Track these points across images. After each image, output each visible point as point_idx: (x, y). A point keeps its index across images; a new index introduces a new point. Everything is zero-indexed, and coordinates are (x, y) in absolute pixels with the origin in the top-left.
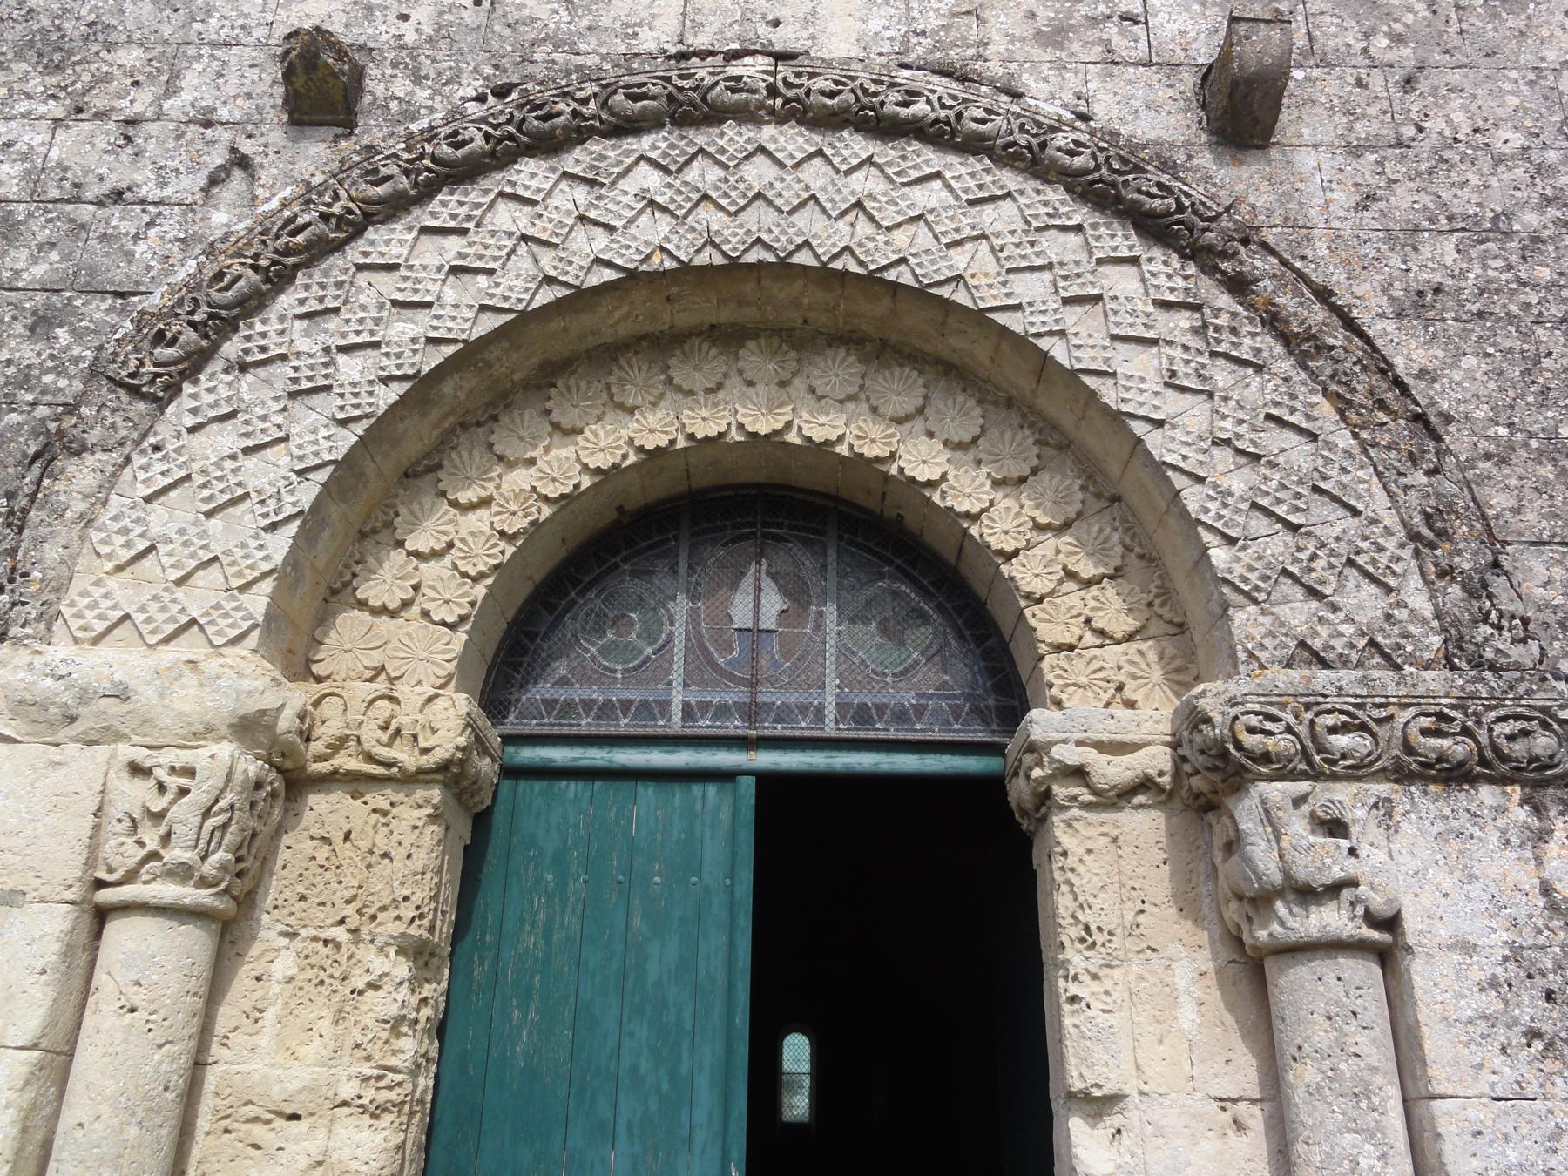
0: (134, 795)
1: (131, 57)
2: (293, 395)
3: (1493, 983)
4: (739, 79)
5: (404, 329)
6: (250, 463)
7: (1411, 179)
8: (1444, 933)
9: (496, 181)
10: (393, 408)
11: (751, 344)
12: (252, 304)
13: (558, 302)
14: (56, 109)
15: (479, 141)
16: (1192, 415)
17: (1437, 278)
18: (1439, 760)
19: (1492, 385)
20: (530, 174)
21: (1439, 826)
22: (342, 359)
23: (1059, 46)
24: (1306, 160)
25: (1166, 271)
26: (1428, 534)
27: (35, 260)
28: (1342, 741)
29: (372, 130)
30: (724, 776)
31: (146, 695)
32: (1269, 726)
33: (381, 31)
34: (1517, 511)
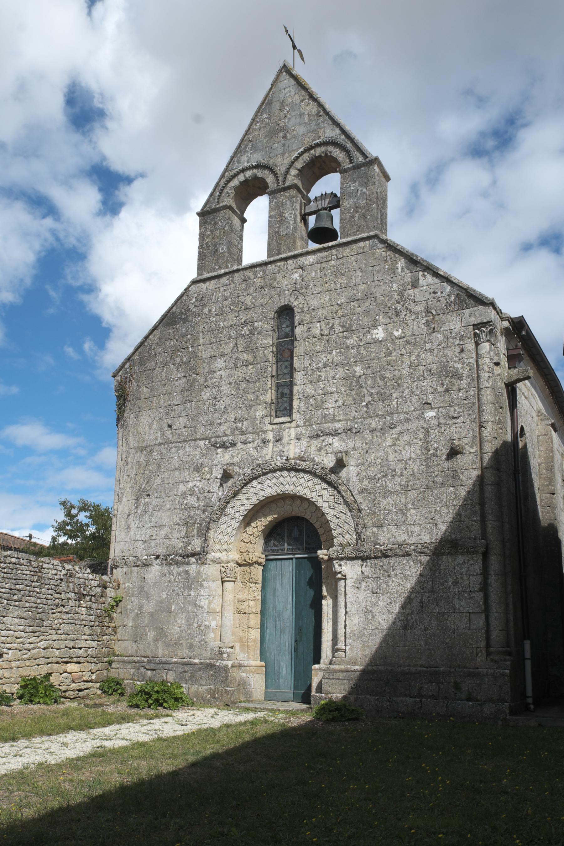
0: (223, 569)
5: (243, 508)
6: (228, 529)
8: (350, 577)
9: (250, 485)
12: (225, 507)
14: (199, 479)
16: (332, 512)
17: (364, 487)
20: (254, 483)
23: (320, 451)
25: (330, 490)
28: (340, 556)
30: (291, 559)
31: (222, 558)
33: (236, 460)
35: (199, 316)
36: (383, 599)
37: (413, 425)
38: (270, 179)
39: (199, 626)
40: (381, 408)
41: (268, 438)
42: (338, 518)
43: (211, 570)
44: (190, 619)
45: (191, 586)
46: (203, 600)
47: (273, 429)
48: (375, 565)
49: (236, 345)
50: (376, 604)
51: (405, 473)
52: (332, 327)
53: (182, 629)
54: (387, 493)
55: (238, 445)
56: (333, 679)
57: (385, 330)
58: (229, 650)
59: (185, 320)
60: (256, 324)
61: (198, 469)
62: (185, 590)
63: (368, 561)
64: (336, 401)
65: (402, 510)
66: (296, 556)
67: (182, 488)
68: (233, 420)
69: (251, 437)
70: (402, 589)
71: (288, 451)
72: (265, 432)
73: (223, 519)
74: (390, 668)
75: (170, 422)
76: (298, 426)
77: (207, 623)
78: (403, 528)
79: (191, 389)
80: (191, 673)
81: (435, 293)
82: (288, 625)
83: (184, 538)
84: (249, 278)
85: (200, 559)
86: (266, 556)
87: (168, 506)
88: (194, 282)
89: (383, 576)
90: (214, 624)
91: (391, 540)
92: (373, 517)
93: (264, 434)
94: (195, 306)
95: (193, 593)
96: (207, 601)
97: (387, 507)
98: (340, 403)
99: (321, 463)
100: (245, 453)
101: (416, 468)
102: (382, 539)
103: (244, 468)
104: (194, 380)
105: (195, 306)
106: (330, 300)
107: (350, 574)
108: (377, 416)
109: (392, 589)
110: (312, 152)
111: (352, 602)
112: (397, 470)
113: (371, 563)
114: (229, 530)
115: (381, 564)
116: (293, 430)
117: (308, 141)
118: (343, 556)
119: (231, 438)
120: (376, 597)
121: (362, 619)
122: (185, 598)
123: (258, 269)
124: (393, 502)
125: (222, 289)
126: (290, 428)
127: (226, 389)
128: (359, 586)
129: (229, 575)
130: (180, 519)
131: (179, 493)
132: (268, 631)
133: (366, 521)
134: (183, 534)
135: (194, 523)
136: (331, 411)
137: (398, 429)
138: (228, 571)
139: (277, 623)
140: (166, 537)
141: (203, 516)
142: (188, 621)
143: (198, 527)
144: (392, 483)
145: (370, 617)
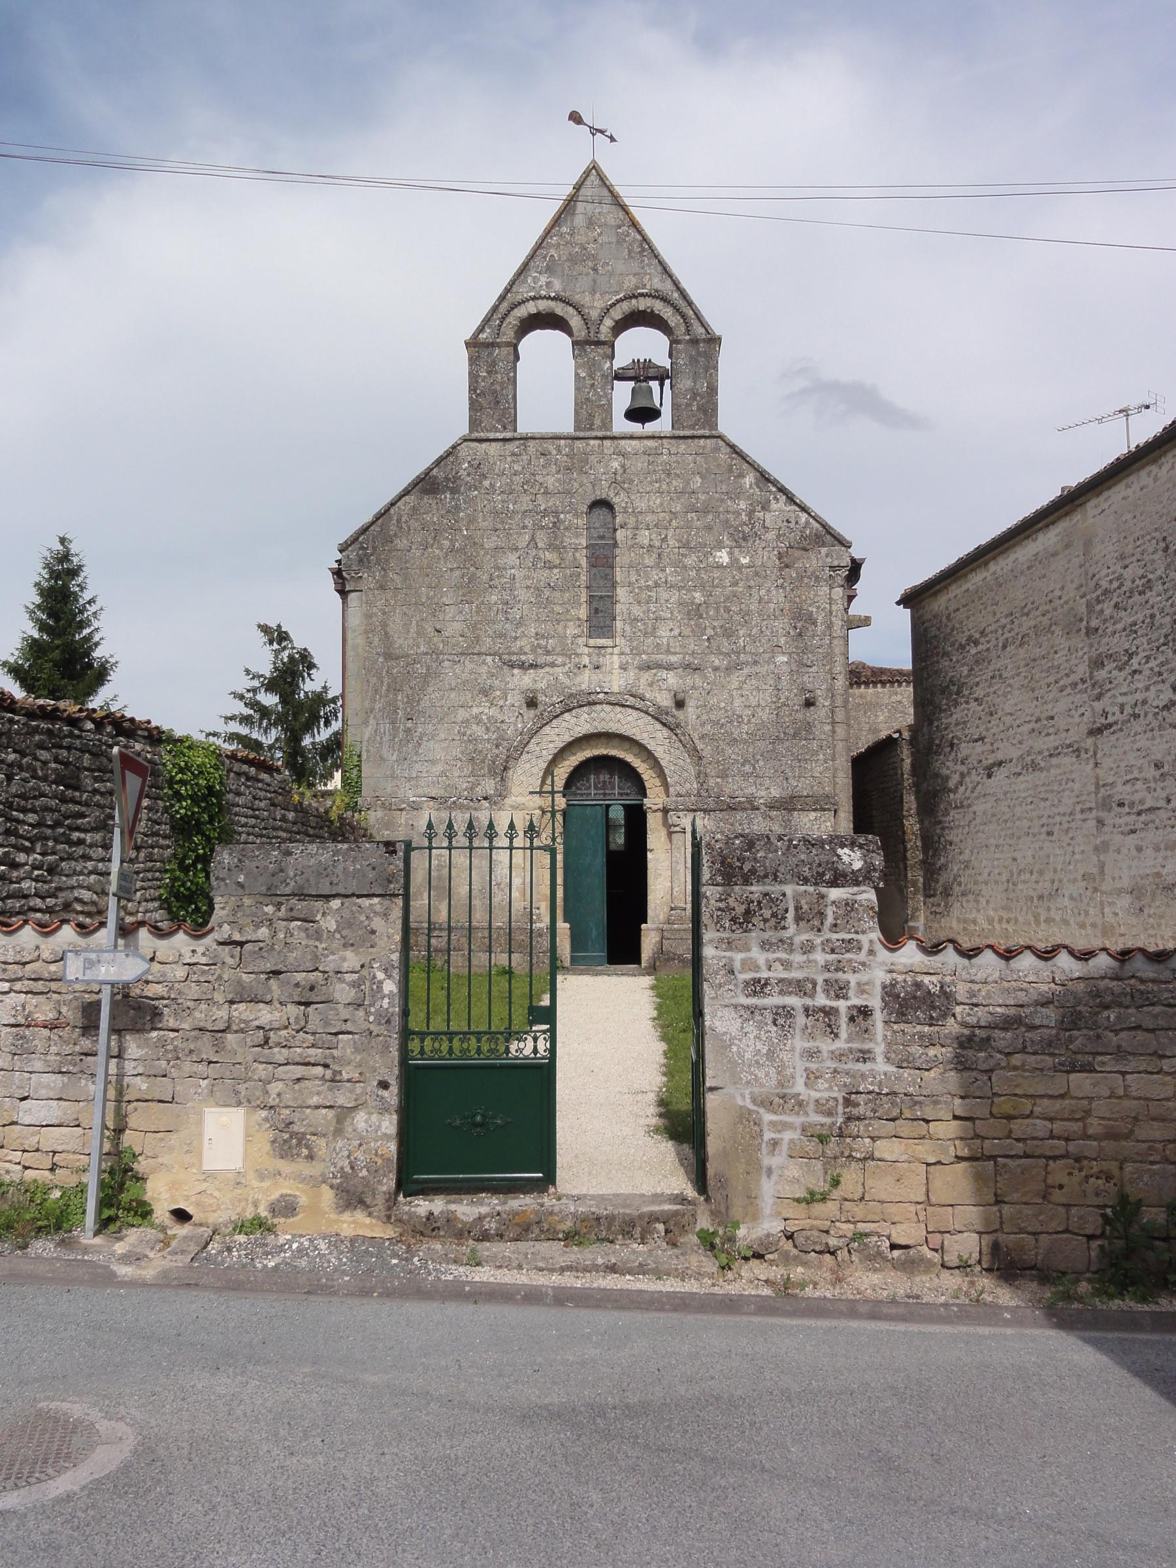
1: (498, 693)
5: (551, 745)
16: (668, 757)
20: (567, 716)
24: (690, 709)
25: (666, 732)
26: (698, 776)
29: (541, 708)
35: (476, 489)
37: (762, 669)
38: (575, 322)
40: (726, 646)
49: (533, 538)
51: (753, 720)
52: (664, 540)
57: (730, 554)
59: (454, 491)
60: (562, 516)
61: (485, 692)
64: (671, 630)
67: (462, 714)
69: (560, 660)
72: (577, 655)
73: (525, 757)
75: (438, 627)
76: (622, 653)
79: (469, 589)
81: (788, 521)
84: (550, 453)
87: (443, 736)
88: (465, 440)
94: (469, 475)
98: (676, 632)
101: (765, 717)
104: (474, 575)
105: (469, 475)
106: (661, 504)
108: (721, 653)
110: (634, 301)
116: (615, 657)
117: (630, 283)
123: (562, 442)
125: (509, 459)
126: (612, 654)
127: (522, 594)
130: (462, 753)
134: (466, 772)
136: (665, 641)
137: (746, 671)
140: (443, 774)
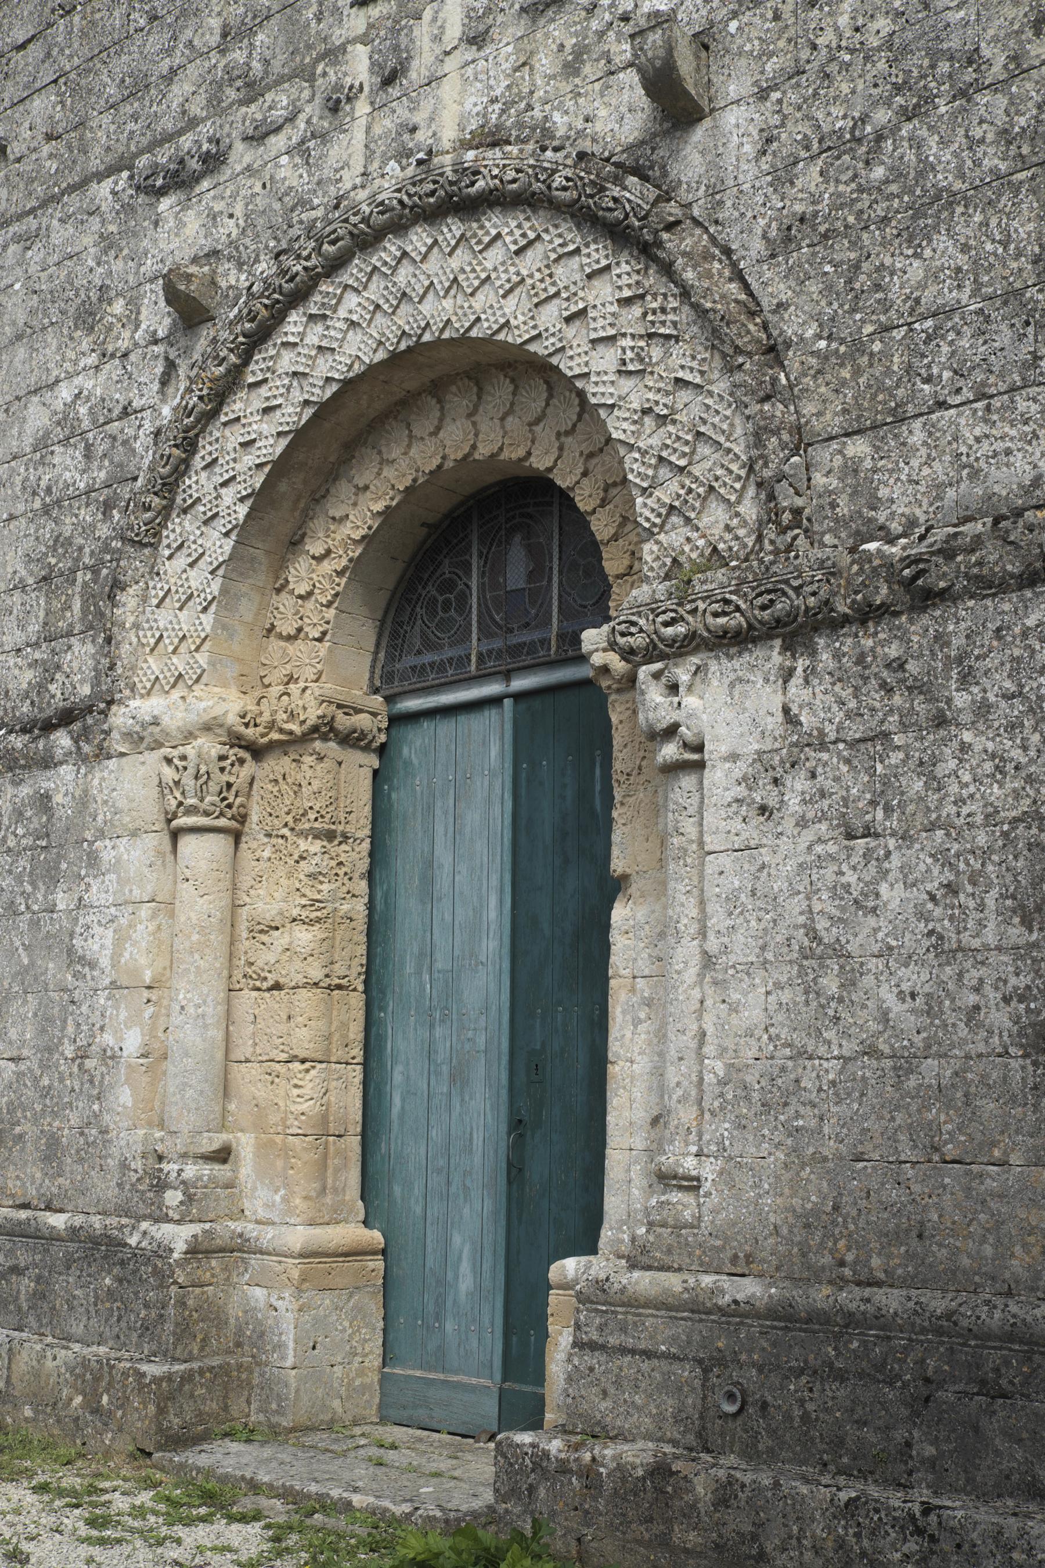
0: (169, 774)
2: (206, 523)
3: (745, 778)
4: (382, 203)
7: (799, 108)
8: (724, 749)
10: (248, 516)
11: (454, 389)
13: (315, 415)
15: (264, 312)
16: (636, 394)
17: (799, 208)
18: (726, 633)
19: (823, 303)
20: (295, 319)
21: (733, 676)
22: (223, 491)
23: (577, 73)
25: (626, 270)
27: (100, 469)
28: (669, 631)
30: (495, 701)
32: (633, 630)
34: (820, 414)
36: (905, 870)
39: (82, 1055)
41: (348, 81)
42: (662, 420)
43: (129, 784)
44: (50, 1020)
45: (57, 868)
46: (97, 930)
47: (371, 26)
48: (860, 660)
50: (866, 903)
53: (23, 1067)
54: (928, 208)
55: (232, 158)
56: (624, 1351)
58: (191, 1171)
62: (35, 887)
63: (821, 642)
65: (1018, 293)
66: (521, 683)
68: (214, 39)
70: (1017, 795)
71: (432, 119)
74: (938, 1303)
77: (108, 1039)
78: (1022, 405)
80: (38, 1279)
82: (481, 1041)
83: (36, 645)
85: (85, 734)
86: (389, 699)
89: (904, 728)
90: (132, 1041)
91: (951, 493)
92: (846, 373)
93: (335, 63)
95: (62, 901)
96: (110, 933)
97: (927, 296)
99: (581, 134)
100: (258, 188)
102: (900, 499)
103: (257, 260)
107: (722, 730)
109: (960, 801)
111: (732, 899)
112: (986, 52)
113: (837, 656)
114: (196, 578)
115: (893, 651)
118: (681, 629)
119: (206, 129)
120: (867, 855)
121: (786, 996)
122: (35, 924)
124: (962, 260)
128: (772, 802)
129: (192, 801)
130: (28, 559)
131: (28, 441)
132: (398, 1078)
133: (809, 409)
135: (73, 571)
138: (188, 781)
139: (438, 1032)
141: (104, 531)
142: (43, 1031)
143: (85, 584)
144: (960, 139)
145: (831, 984)
